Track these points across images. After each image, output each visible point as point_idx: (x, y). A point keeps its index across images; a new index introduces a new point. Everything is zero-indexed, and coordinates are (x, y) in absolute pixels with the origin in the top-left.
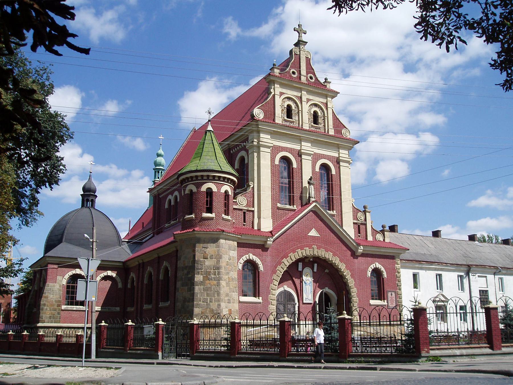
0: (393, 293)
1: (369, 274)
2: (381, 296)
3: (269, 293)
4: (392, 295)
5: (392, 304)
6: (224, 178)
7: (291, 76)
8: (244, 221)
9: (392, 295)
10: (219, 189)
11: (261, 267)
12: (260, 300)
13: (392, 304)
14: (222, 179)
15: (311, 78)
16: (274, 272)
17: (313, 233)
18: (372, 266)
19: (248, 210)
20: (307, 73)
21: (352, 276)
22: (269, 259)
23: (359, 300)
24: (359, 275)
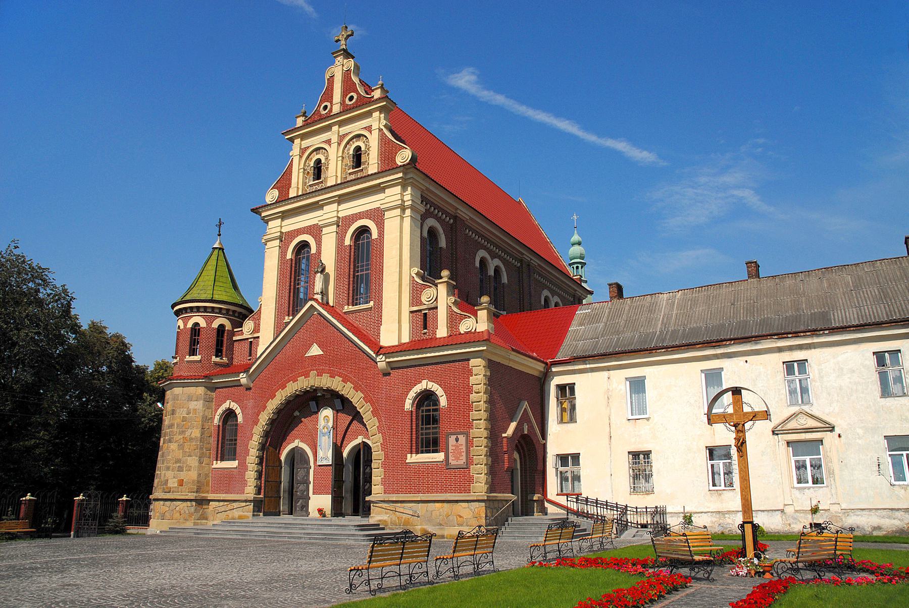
0: (462, 439)
1: (408, 405)
2: (431, 444)
3: (247, 453)
4: (457, 440)
5: (457, 459)
6: (191, 308)
7: (321, 115)
8: (250, 355)
9: (457, 440)
10: (185, 325)
11: (240, 419)
12: (235, 464)
13: (457, 459)
14: (195, 310)
15: (351, 98)
16: (256, 422)
17: (315, 350)
18: (232, 403)
19: (254, 338)
20: (344, 95)
21: (375, 413)
22: (250, 403)
23: (386, 456)
24: (387, 410)
